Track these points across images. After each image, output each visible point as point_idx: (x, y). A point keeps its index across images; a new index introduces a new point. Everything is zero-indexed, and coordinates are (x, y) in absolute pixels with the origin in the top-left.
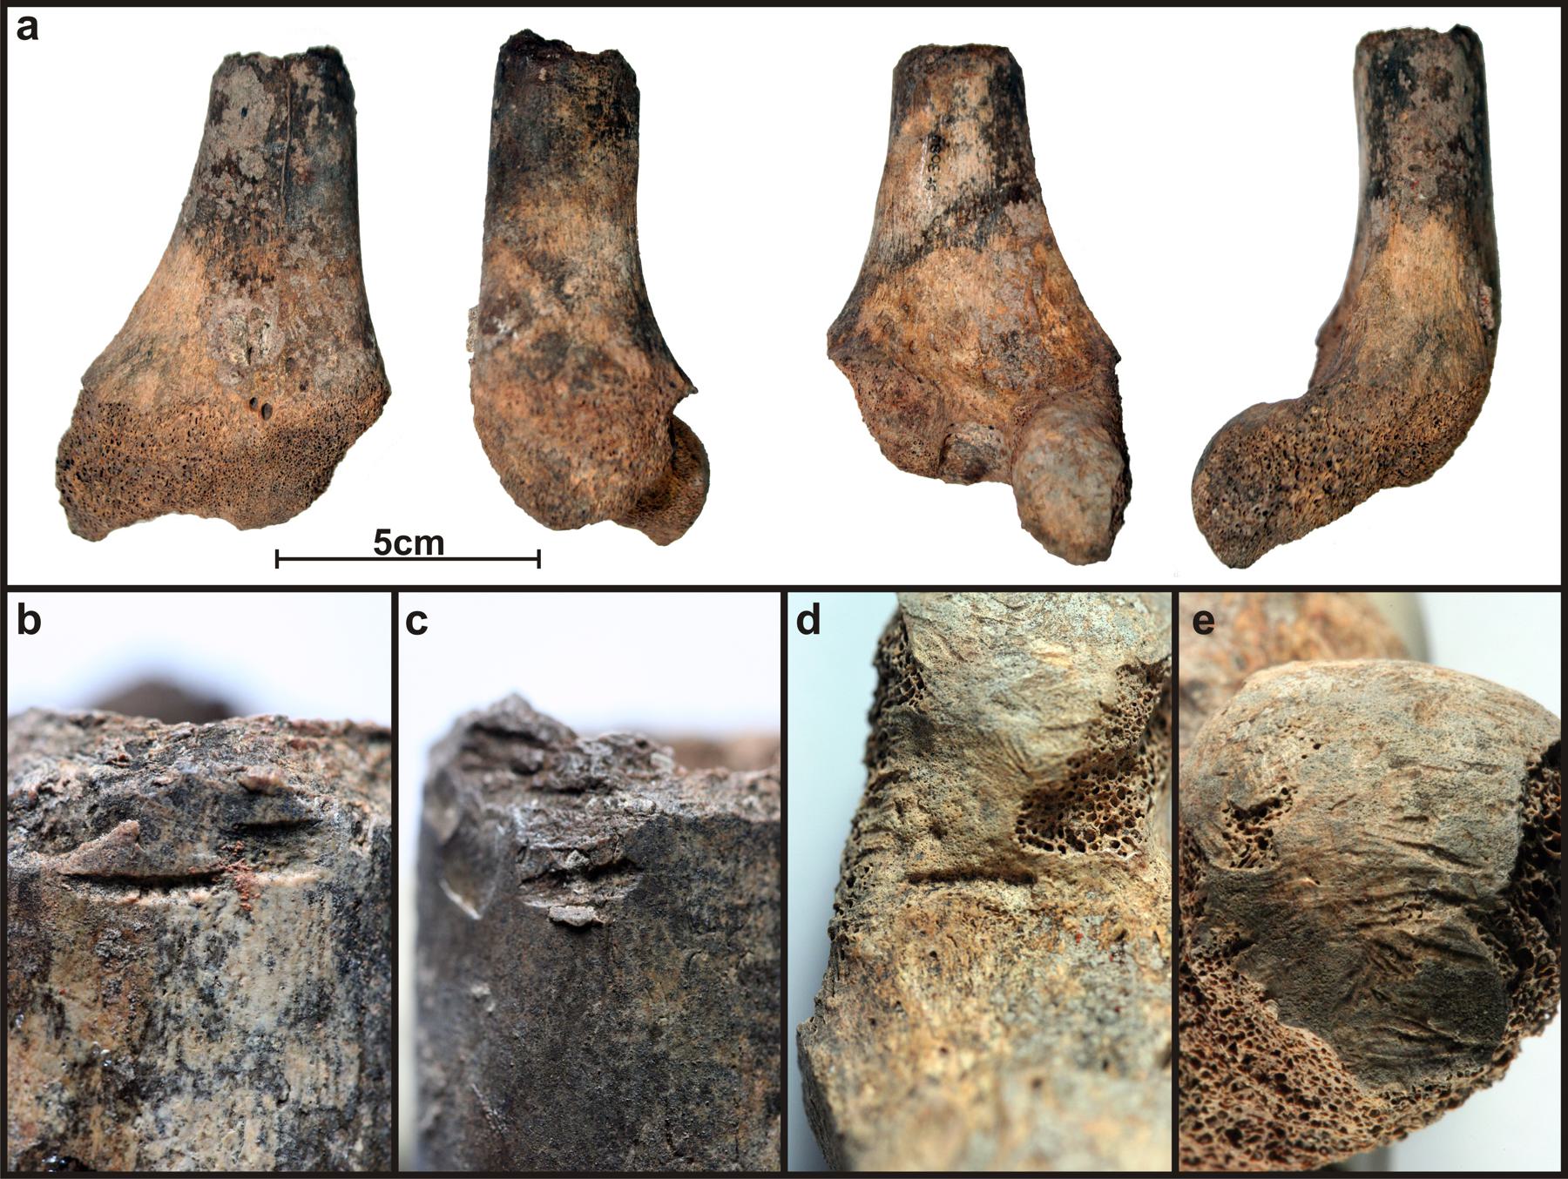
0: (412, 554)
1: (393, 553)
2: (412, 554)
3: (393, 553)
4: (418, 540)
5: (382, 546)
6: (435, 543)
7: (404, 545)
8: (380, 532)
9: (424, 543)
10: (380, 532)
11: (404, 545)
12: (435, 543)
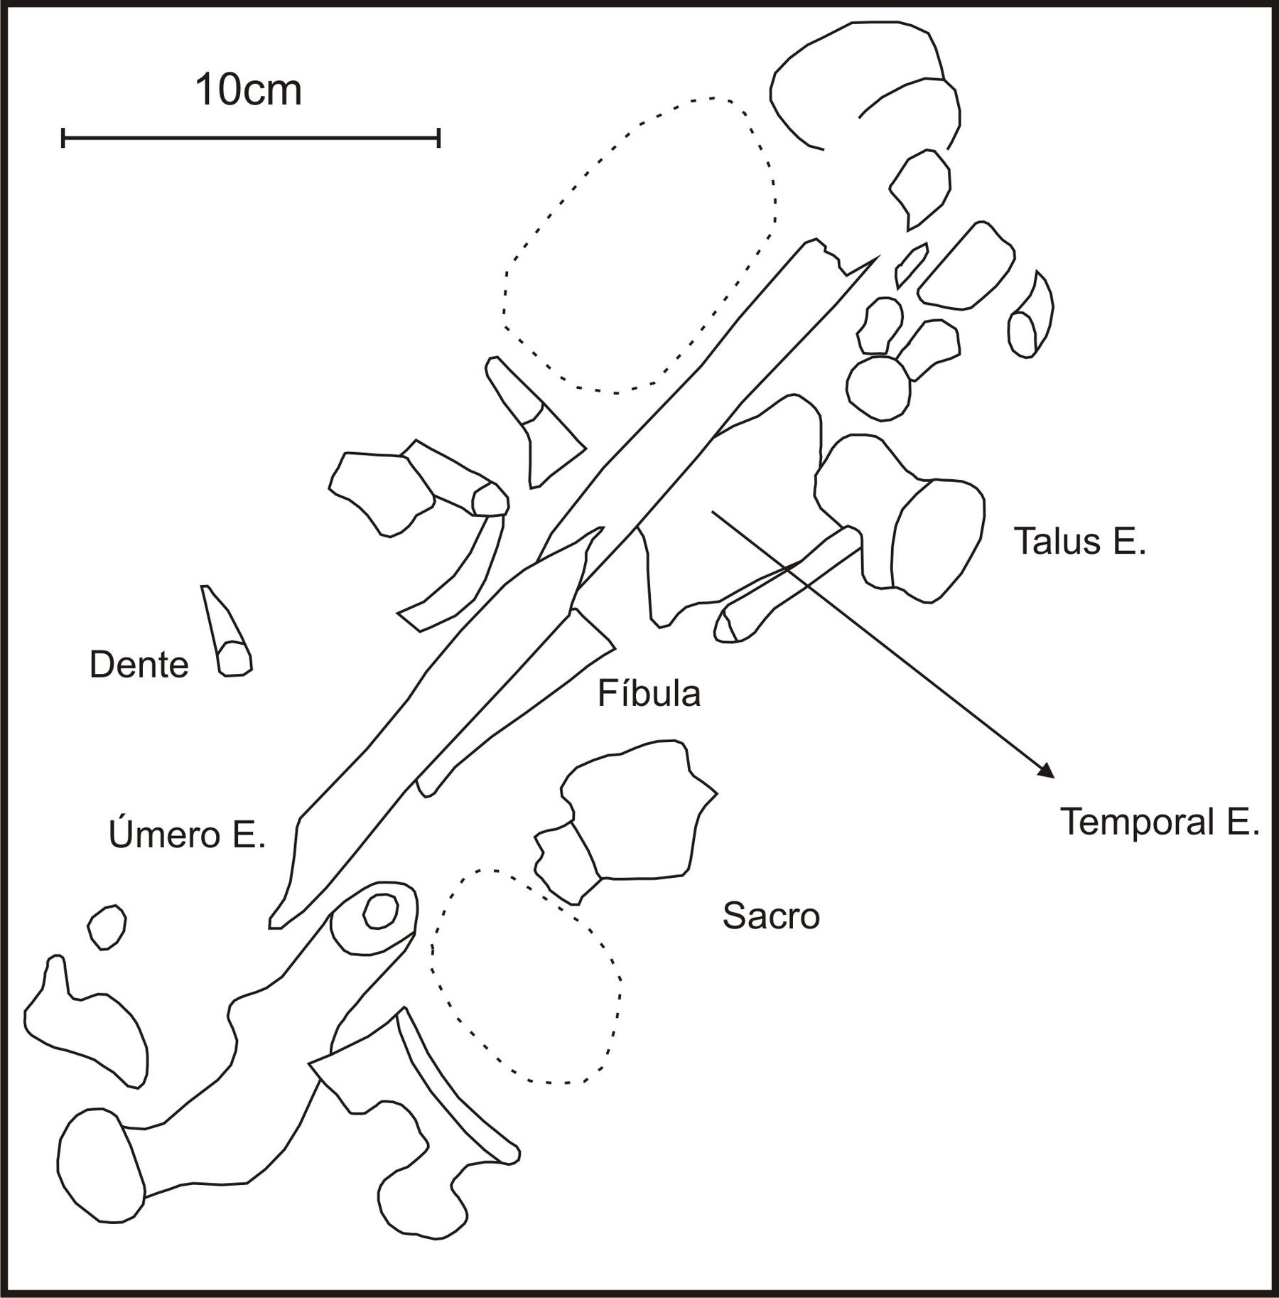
4: (271, 85)
6: (291, 90)
7: (255, 93)
9: (278, 90)
11: (255, 93)
12: (291, 90)
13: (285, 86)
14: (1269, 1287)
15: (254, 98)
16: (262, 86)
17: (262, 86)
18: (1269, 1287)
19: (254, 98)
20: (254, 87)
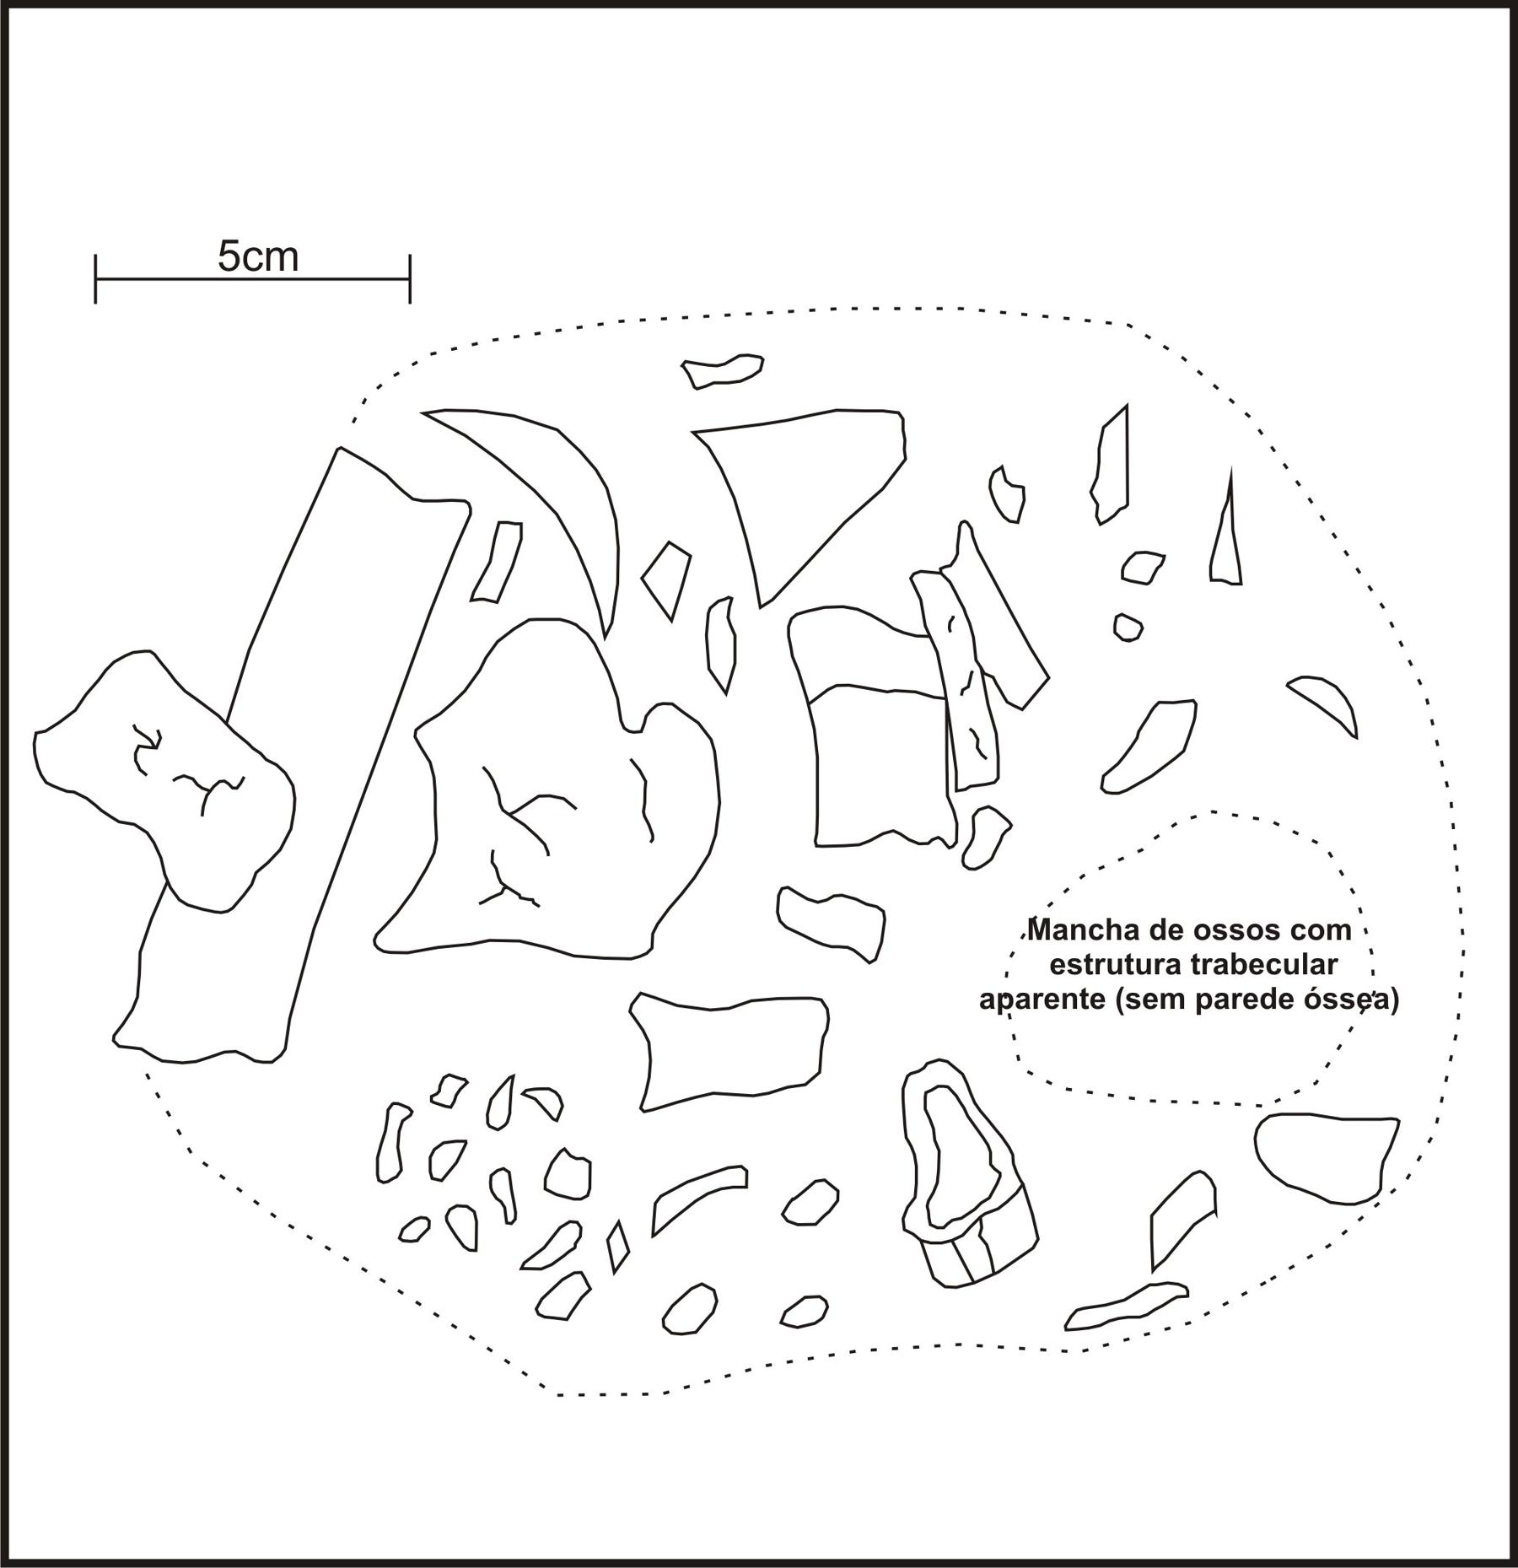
0: (263, 273)
1: (241, 271)
2: (263, 273)
3: (241, 271)
4: (269, 252)
5: (229, 260)
6: (289, 256)
8: (225, 242)
9: (275, 256)
10: (225, 242)
12: (289, 256)
13: (282, 253)
14: (1506, 1555)
15: (253, 263)
16: (260, 253)
17: (260, 253)
18: (1506, 1555)
19: (253, 263)
20: (253, 256)
